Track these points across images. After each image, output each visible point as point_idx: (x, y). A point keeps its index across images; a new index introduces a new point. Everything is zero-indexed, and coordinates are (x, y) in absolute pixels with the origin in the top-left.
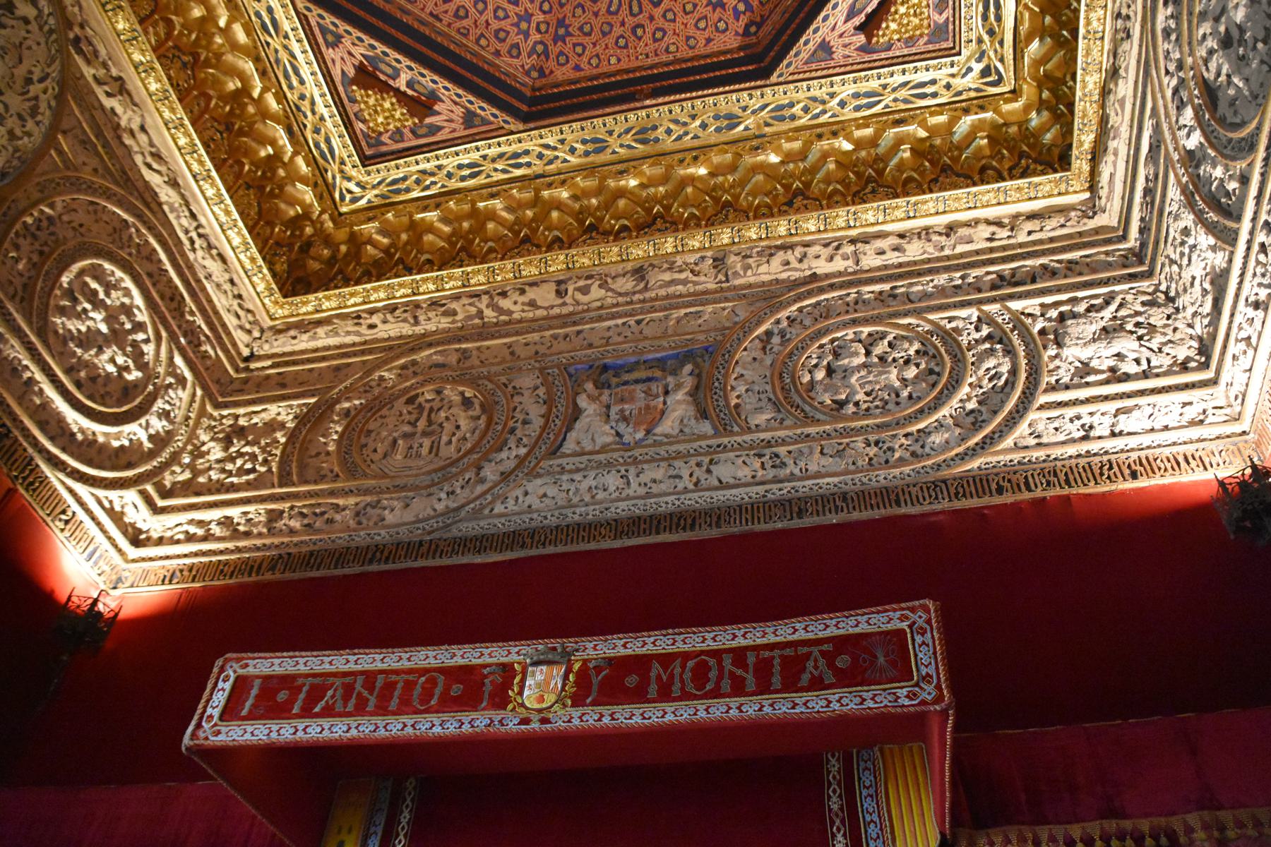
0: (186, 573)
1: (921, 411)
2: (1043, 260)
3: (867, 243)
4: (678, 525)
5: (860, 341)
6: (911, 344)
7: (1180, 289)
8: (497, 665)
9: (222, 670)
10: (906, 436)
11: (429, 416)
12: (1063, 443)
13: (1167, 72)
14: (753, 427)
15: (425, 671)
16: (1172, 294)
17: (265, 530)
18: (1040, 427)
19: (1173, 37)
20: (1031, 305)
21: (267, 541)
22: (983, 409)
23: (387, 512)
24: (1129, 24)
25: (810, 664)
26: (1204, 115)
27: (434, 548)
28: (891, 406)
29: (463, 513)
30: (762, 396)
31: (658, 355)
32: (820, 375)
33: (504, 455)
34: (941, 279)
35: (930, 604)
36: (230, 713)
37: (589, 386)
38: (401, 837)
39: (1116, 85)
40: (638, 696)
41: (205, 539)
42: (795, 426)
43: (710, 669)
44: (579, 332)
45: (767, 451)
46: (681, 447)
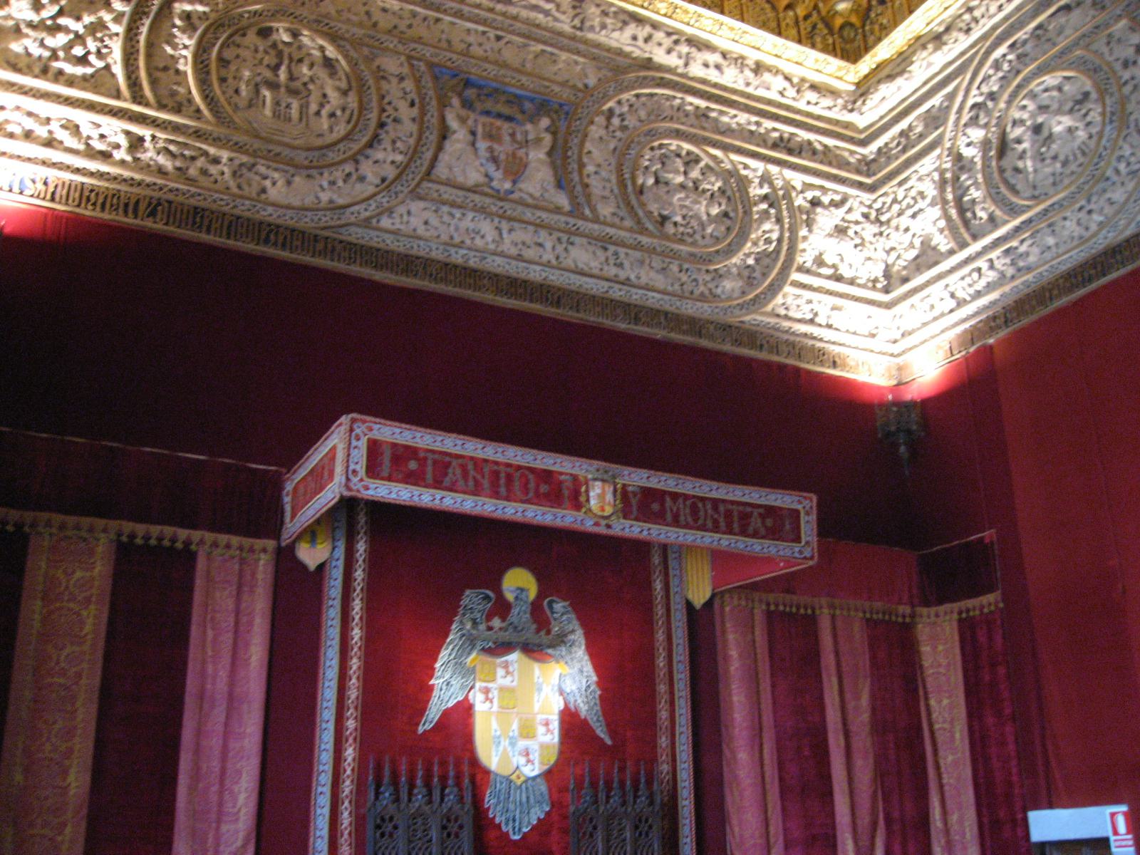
0: (40, 186)
1: (717, 252)
2: (812, 137)
3: (699, 50)
4: (547, 300)
5: (679, 156)
6: (717, 180)
7: (894, 223)
8: (571, 475)
10: (707, 271)
11: (289, 67)
12: (800, 321)
13: (979, 88)
14: (602, 218)
15: (519, 468)
16: (883, 218)
17: (129, 158)
18: (789, 300)
19: (1000, 74)
20: (797, 179)
21: (137, 176)
22: (757, 268)
23: (268, 183)
24: (973, 25)
26: (990, 149)
27: (330, 246)
28: (698, 237)
29: (349, 216)
30: (608, 185)
31: (519, 92)
32: (651, 181)
33: (380, 155)
34: (743, 118)
37: (456, 101)
39: (936, 49)
40: (659, 518)
41: (50, 143)
42: (631, 230)
44: (438, 20)
45: (612, 248)
46: (544, 215)
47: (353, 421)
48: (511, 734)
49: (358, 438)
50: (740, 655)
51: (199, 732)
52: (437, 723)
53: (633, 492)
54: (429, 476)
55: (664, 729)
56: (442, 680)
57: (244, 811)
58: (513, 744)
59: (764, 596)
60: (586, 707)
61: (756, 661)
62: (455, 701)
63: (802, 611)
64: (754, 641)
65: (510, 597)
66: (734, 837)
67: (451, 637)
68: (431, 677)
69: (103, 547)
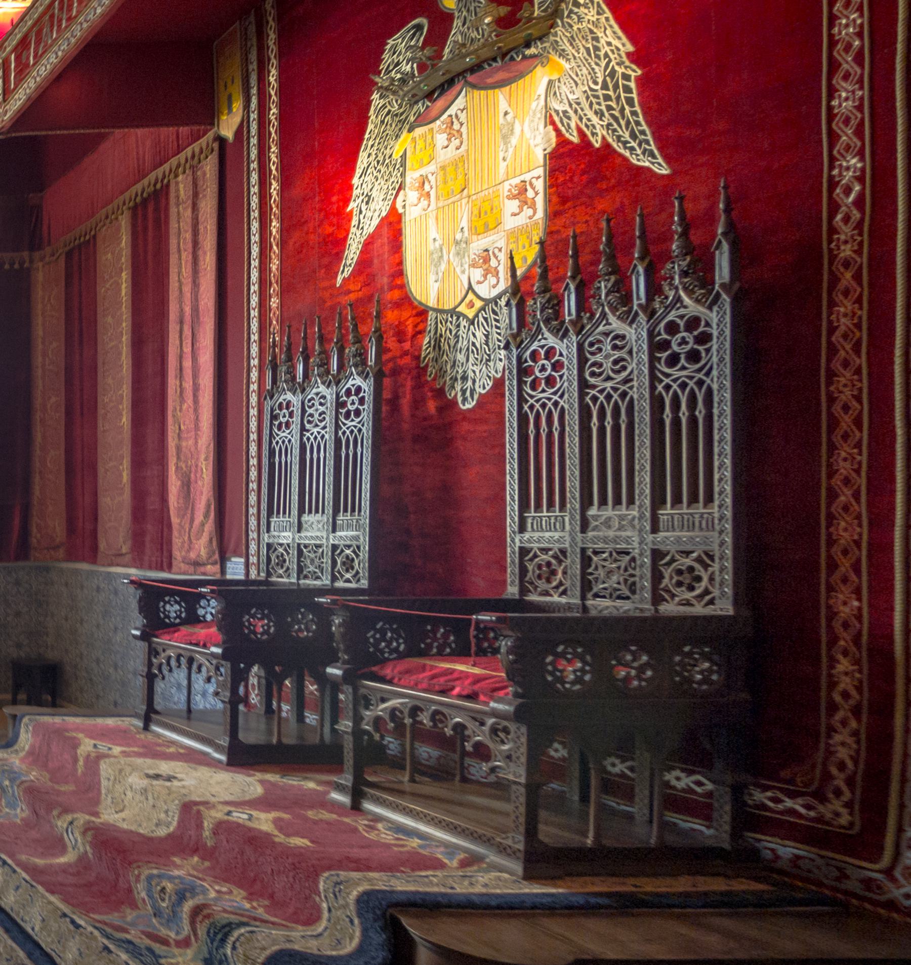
48: (459, 236)
52: (357, 263)
56: (361, 198)
60: (607, 118)
67: (370, 127)
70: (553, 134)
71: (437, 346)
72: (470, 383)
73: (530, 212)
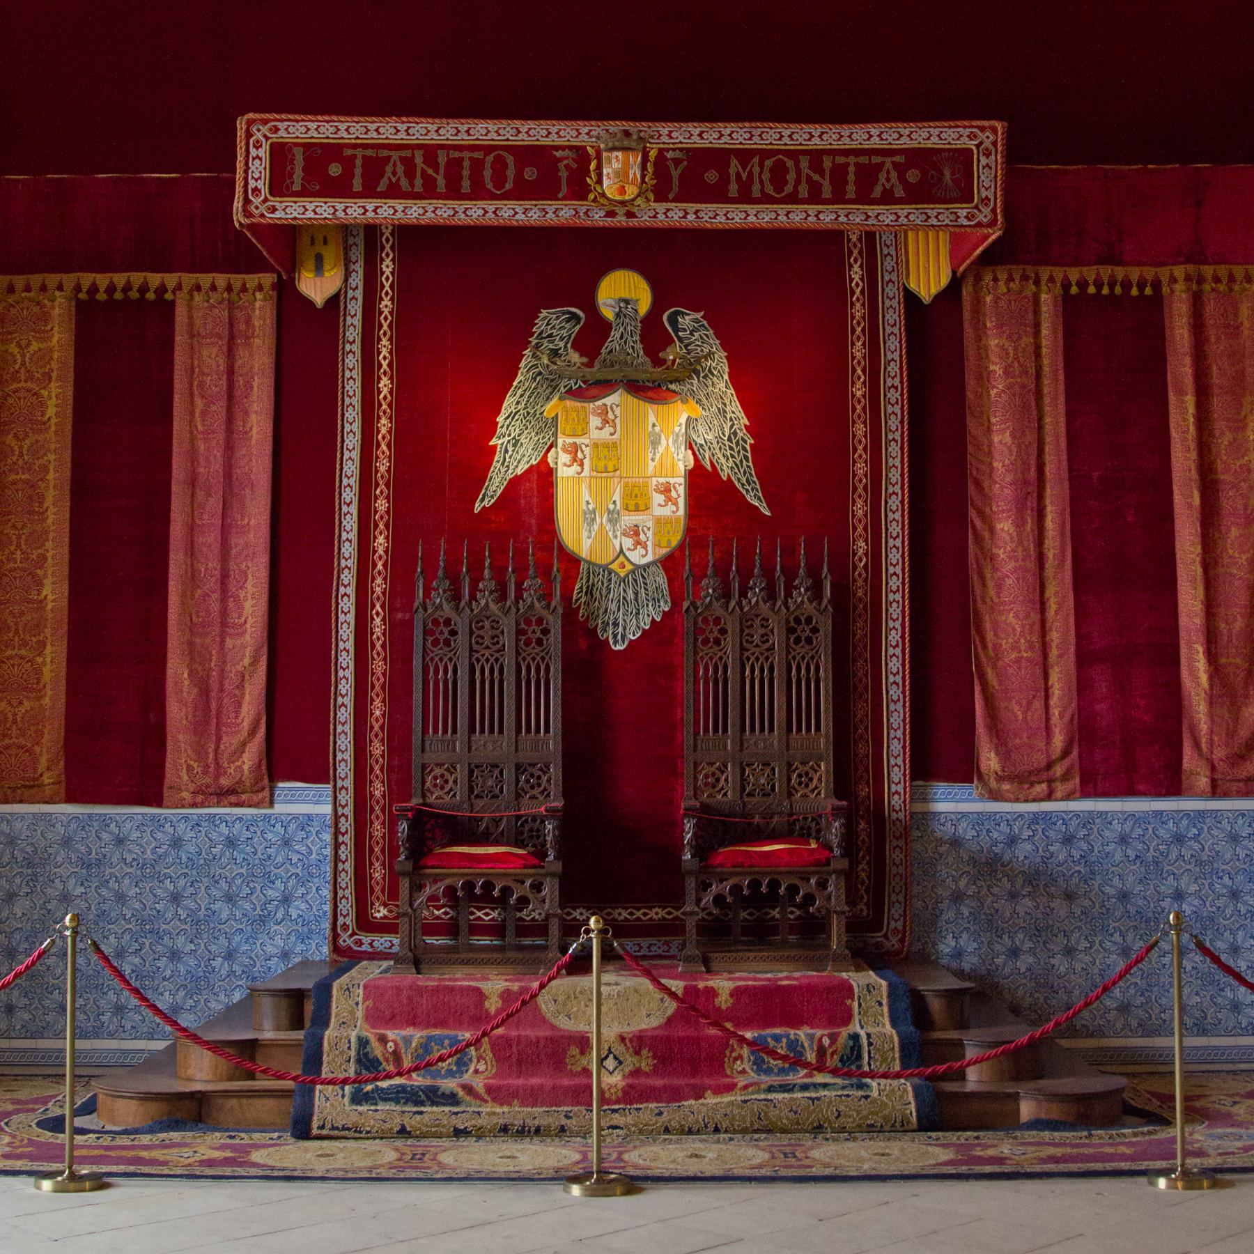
8: (571, 148)
9: (249, 135)
15: (489, 149)
25: (882, 176)
35: (999, 125)
36: (279, 186)
38: (388, 249)
40: (718, 195)
43: (787, 170)
47: (250, 123)
48: (611, 507)
49: (258, 146)
50: (1006, 373)
51: (192, 528)
53: (674, 160)
54: (357, 185)
55: (860, 490)
56: (507, 439)
57: (250, 621)
58: (614, 518)
59: (1059, 273)
60: (731, 464)
61: (1038, 376)
62: (527, 467)
63: (1134, 292)
64: (1038, 347)
65: (608, 314)
66: (985, 647)
67: (519, 378)
68: (492, 433)
69: (59, 308)
70: (692, 458)
71: (590, 591)
72: (620, 629)
73: (674, 508)
